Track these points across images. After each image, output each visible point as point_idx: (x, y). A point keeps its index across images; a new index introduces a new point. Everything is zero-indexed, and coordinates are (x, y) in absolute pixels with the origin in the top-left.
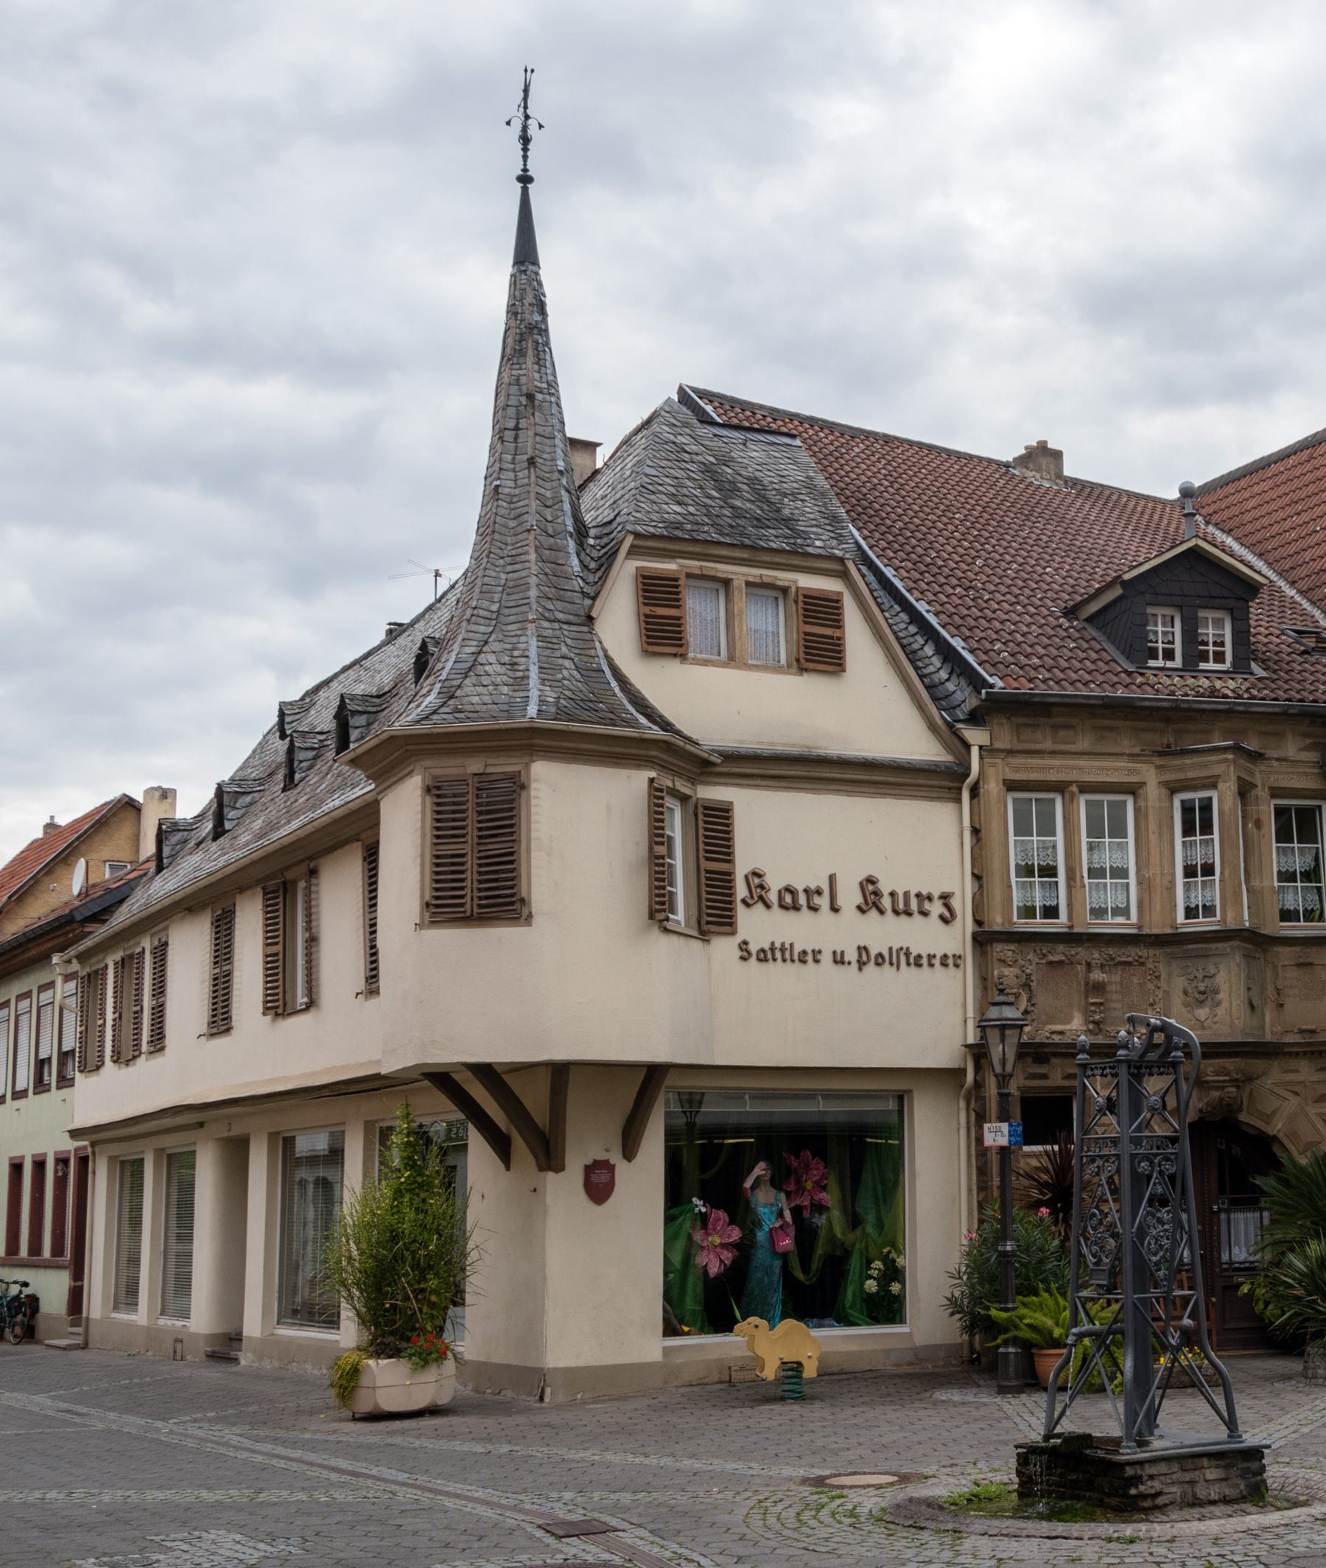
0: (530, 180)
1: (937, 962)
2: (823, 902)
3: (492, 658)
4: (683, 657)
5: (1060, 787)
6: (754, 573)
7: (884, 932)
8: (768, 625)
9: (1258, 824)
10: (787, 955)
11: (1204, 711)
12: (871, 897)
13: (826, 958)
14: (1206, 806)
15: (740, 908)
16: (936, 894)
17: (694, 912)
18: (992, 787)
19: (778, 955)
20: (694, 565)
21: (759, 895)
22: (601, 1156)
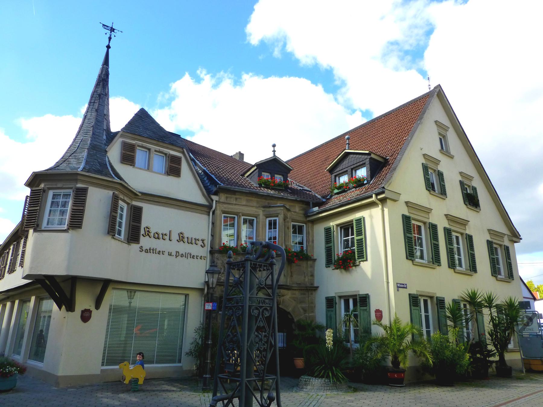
0: (110, 47)
1: (199, 258)
2: (167, 238)
3: (74, 157)
4: (134, 166)
5: (237, 214)
6: (158, 148)
7: (183, 248)
8: (159, 163)
9: (288, 228)
10: (154, 251)
11: (275, 197)
12: (181, 238)
13: (166, 253)
14: (275, 221)
15: (141, 236)
16: (200, 239)
17: (127, 236)
18: (218, 212)
19: (152, 251)
20: (140, 143)
21: (148, 233)
22: (88, 308)
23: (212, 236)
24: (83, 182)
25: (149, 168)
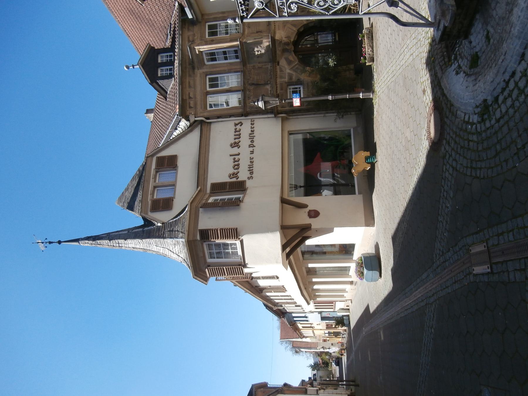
1: (253, 126)
2: (237, 157)
3: (174, 249)
6: (151, 180)
7: (245, 141)
12: (236, 145)
13: (252, 156)
15: (239, 180)
16: (235, 127)
17: (241, 192)
18: (206, 114)
19: (251, 169)
21: (235, 175)
23: (230, 116)
24: (194, 235)
25: (174, 185)
